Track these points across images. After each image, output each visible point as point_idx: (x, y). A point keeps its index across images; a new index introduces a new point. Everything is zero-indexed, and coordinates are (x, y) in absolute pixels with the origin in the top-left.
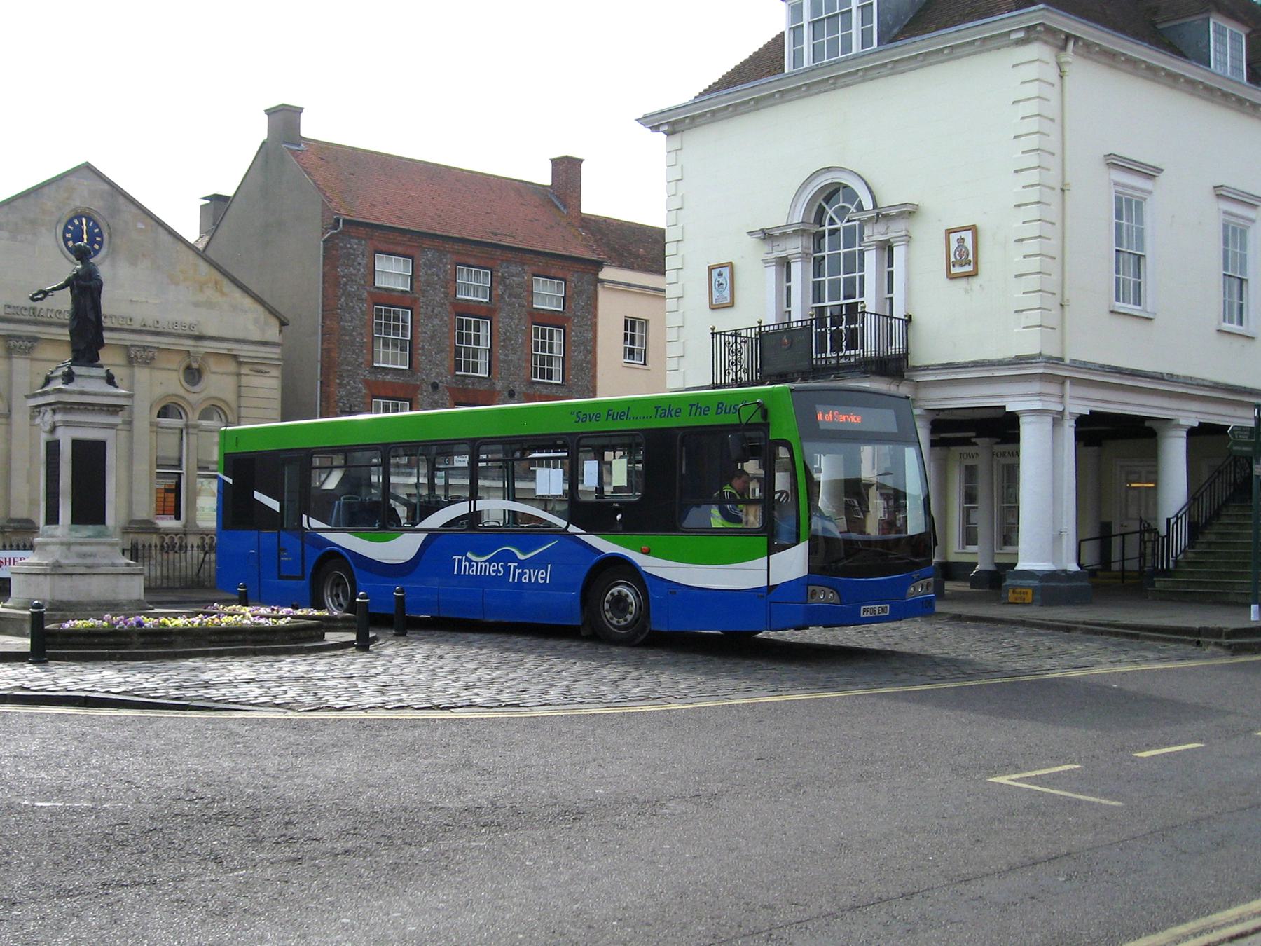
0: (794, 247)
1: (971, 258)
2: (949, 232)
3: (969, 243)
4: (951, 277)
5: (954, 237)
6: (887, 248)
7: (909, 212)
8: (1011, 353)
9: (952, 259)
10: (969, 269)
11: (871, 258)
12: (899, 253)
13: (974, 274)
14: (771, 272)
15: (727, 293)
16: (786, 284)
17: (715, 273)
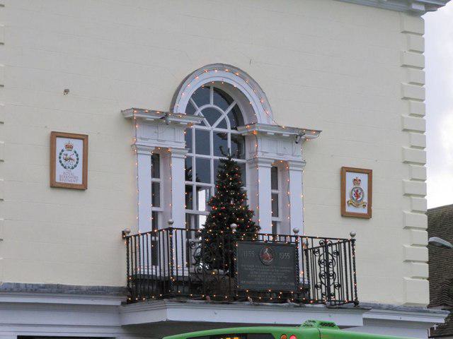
0: (174, 140)
1: (365, 200)
2: (345, 171)
3: (364, 186)
4: (345, 215)
5: (350, 177)
6: (277, 171)
7: (298, 137)
8: (398, 301)
9: (348, 199)
10: (365, 211)
11: (265, 175)
12: (294, 177)
13: (368, 216)
14: (146, 163)
15: (78, 171)
16: (161, 180)
17: (61, 143)
